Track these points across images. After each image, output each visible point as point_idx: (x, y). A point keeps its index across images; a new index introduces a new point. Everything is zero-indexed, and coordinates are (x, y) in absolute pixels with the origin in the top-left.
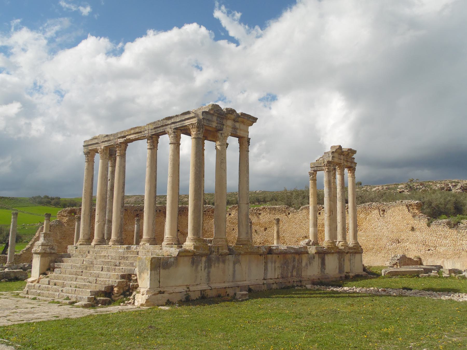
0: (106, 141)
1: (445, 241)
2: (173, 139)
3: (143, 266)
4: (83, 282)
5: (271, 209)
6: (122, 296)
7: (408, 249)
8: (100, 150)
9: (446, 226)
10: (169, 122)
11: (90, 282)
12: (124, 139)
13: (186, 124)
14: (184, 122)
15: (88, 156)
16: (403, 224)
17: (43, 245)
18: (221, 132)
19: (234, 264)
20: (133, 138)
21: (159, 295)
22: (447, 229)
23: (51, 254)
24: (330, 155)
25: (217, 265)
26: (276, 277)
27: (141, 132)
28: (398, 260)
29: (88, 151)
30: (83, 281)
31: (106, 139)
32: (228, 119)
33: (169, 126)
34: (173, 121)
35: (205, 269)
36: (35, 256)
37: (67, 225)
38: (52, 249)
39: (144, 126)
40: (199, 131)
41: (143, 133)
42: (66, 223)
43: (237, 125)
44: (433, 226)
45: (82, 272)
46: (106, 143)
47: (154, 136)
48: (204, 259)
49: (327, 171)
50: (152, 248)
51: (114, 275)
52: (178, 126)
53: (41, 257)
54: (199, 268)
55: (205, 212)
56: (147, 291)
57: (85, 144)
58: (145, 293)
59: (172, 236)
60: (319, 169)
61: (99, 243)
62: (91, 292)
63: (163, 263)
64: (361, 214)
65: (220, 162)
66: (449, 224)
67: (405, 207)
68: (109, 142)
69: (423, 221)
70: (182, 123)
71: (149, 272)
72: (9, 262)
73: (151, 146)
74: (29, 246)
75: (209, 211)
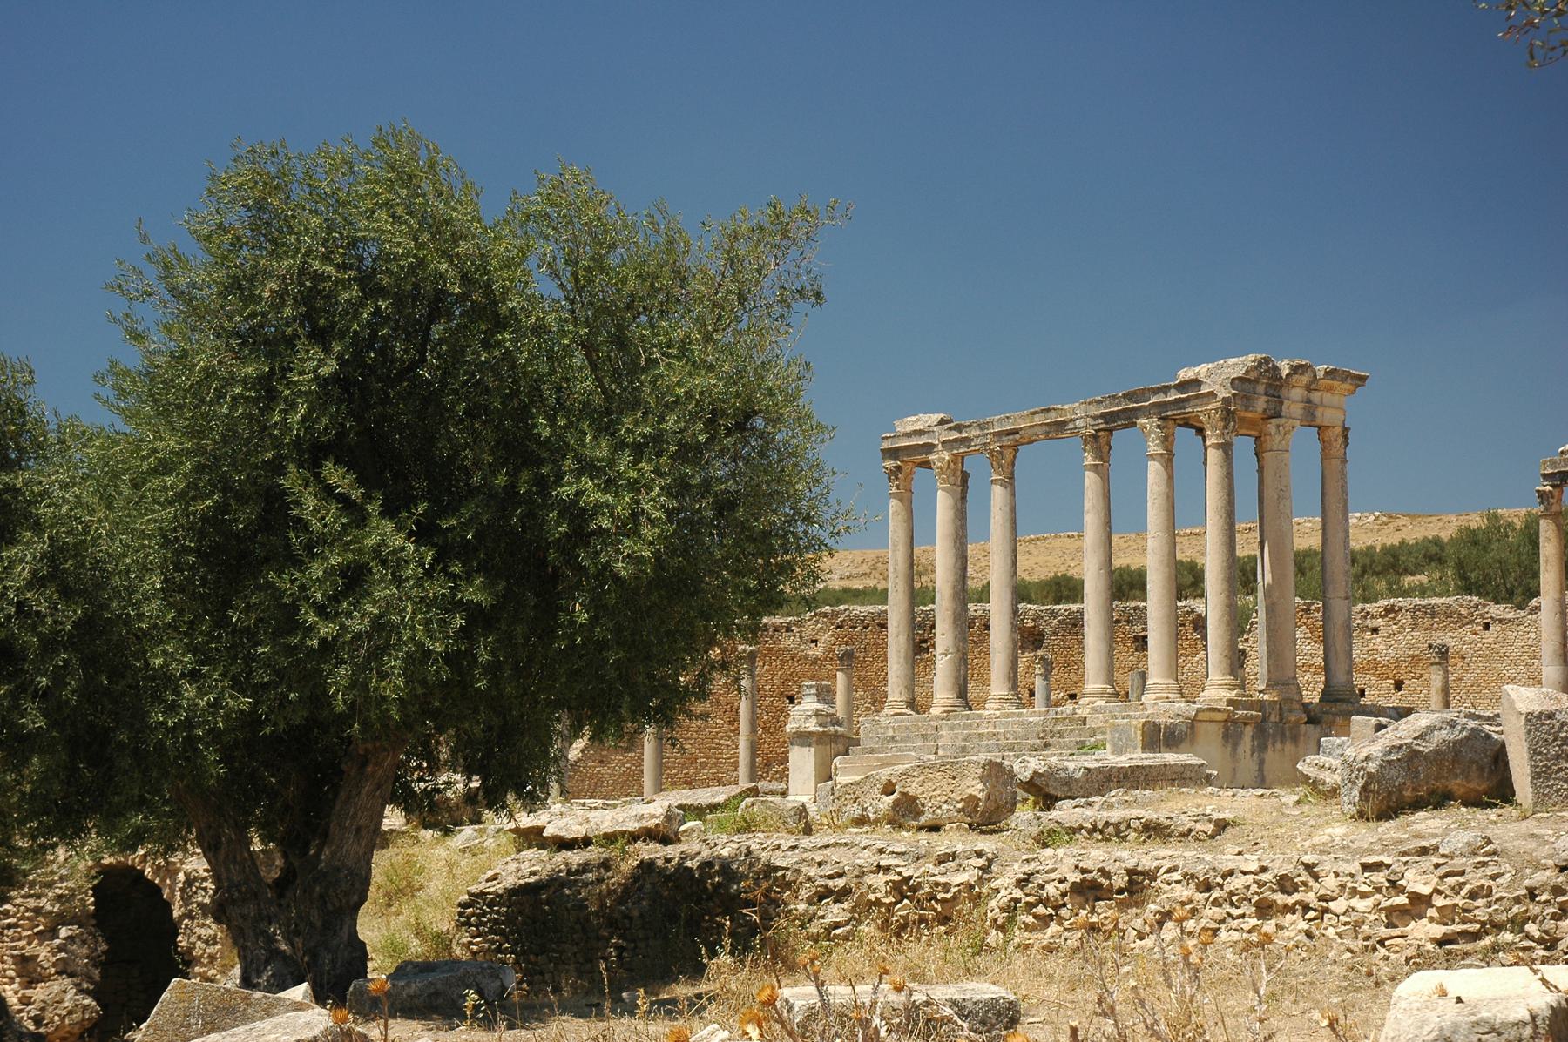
5: (1419, 610)
18: (1274, 421)
25: (1278, 746)
32: (1293, 386)
35: (1252, 755)
40: (1226, 427)
43: (1316, 397)
47: (1101, 434)
48: (1249, 730)
54: (1240, 750)
65: (1276, 497)
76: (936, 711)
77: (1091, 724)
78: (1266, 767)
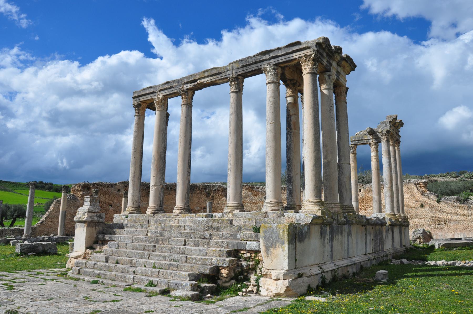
0: (166, 89)
1: (454, 216)
2: (273, 78)
3: (274, 237)
4: (162, 260)
6: (233, 281)
7: (417, 224)
8: (157, 100)
9: (456, 202)
10: (267, 57)
11: (174, 261)
12: (193, 84)
13: (294, 58)
14: (291, 55)
15: (138, 109)
16: (412, 201)
17: (89, 212)
18: (328, 73)
19: (348, 236)
20: (207, 82)
21: (299, 279)
22: (457, 204)
23: (98, 223)
24: (388, 124)
26: (372, 252)
27: (221, 73)
28: (421, 234)
29: (139, 102)
30: (162, 259)
31: (167, 86)
33: (267, 62)
34: (271, 55)
36: (78, 225)
37: (81, 199)
38: (100, 217)
39: (226, 67)
40: (315, 65)
41: (224, 74)
42: (80, 197)
44: (443, 203)
45: (155, 246)
46: (166, 91)
47: (240, 77)
49: (386, 141)
50: (249, 215)
51: (216, 251)
52: (281, 61)
53: (88, 226)
55: (215, 191)
56: (285, 275)
57: (135, 95)
58: (281, 276)
59: (277, 200)
60: (360, 143)
61: (157, 212)
62: (189, 275)
63: (299, 232)
64: (369, 193)
65: (329, 109)
66: (458, 200)
67: (413, 186)
68: (171, 90)
69: (432, 198)
70: (288, 56)
71: (286, 246)
72: (26, 234)
73: (237, 89)
74: (43, 219)
75: (219, 190)
76: (149, 212)
77: (235, 223)
78: (333, 249)
